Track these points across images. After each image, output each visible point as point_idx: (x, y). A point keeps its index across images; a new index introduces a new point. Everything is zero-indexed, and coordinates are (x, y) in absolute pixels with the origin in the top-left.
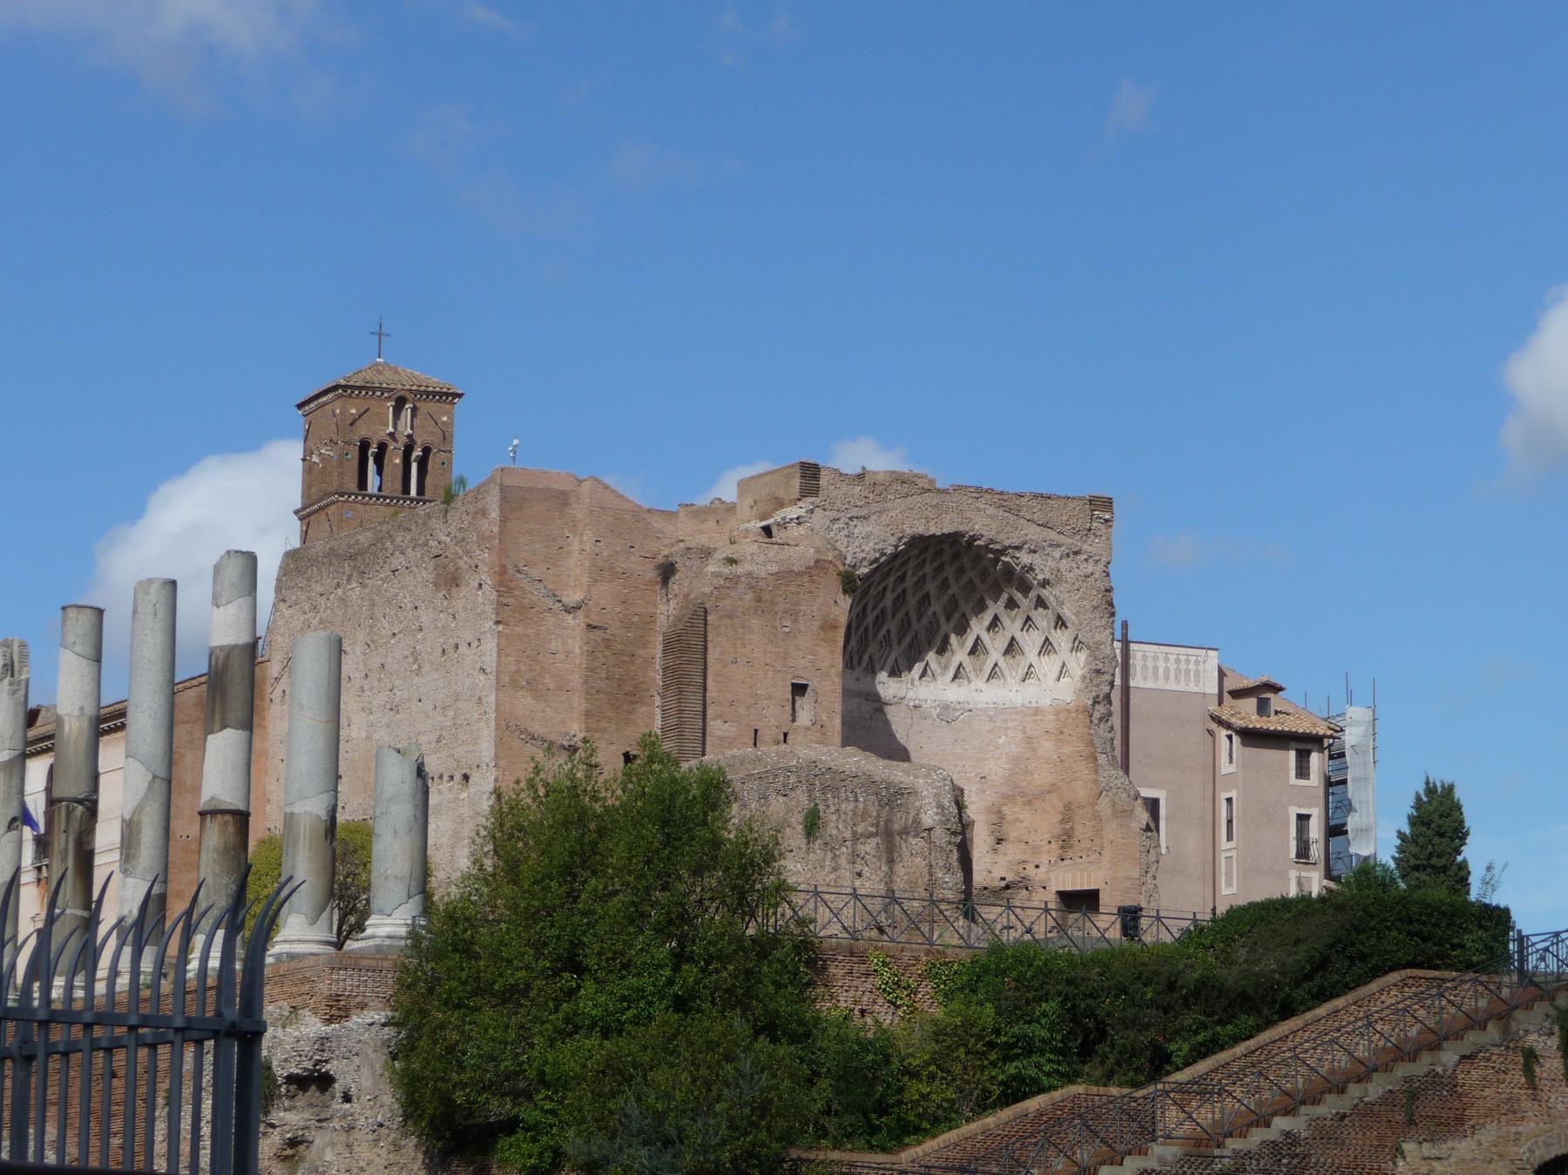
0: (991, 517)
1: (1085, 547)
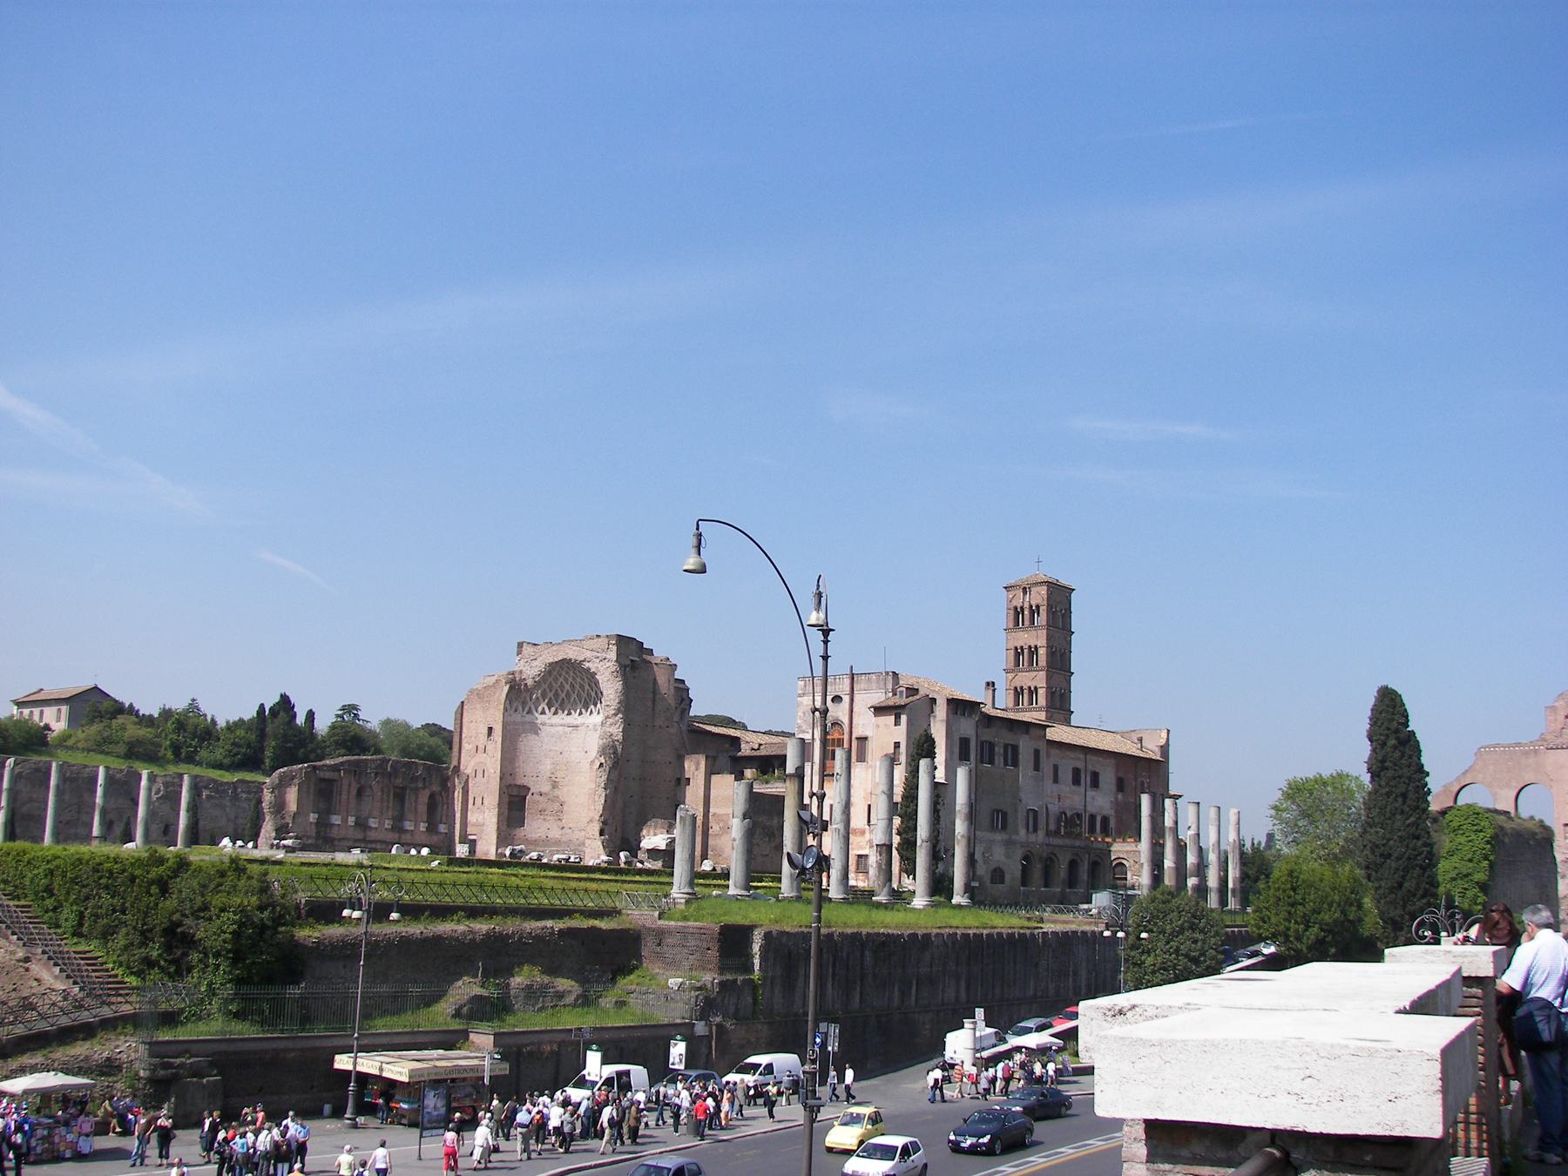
0: (574, 651)
1: (608, 656)
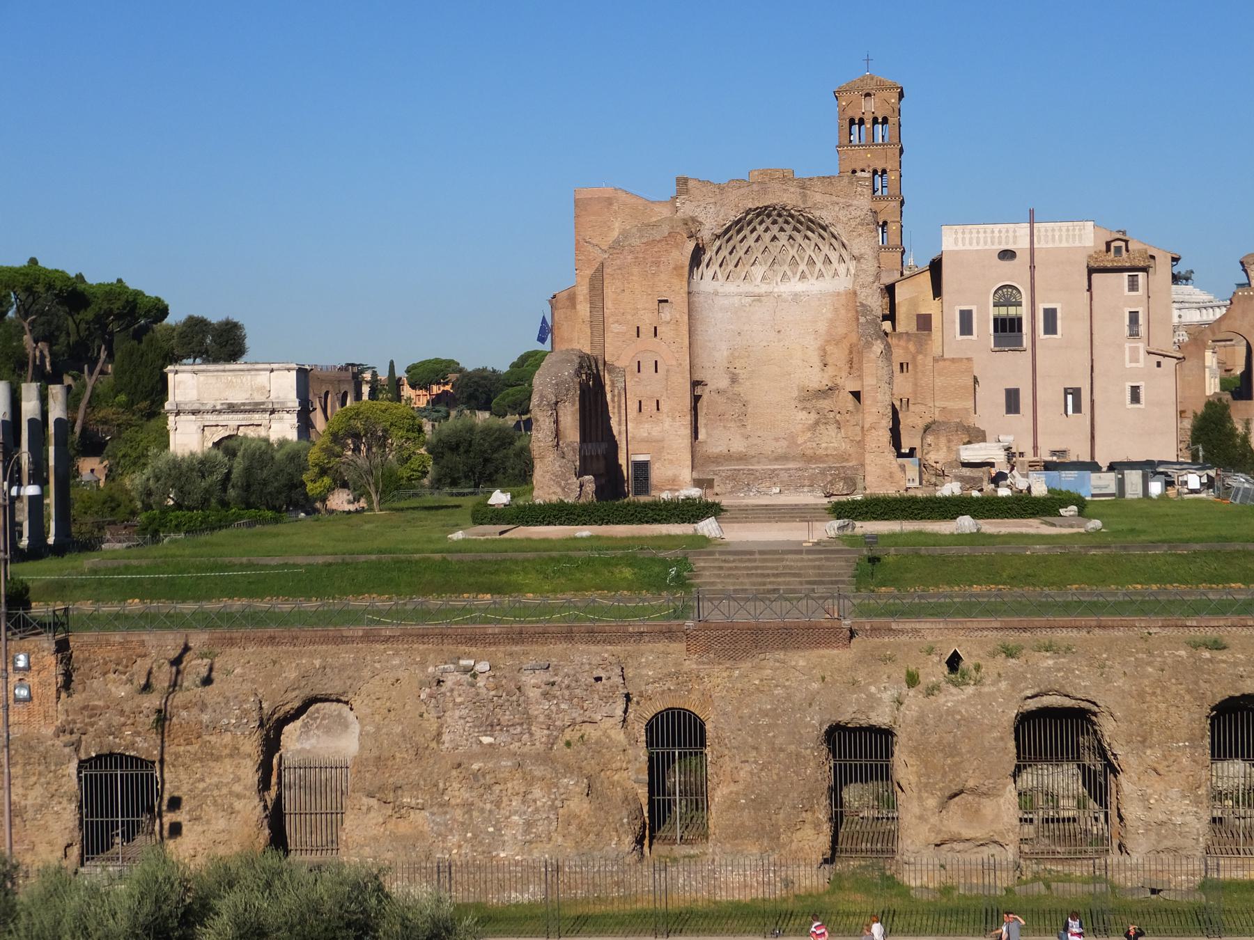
1: (855, 202)
